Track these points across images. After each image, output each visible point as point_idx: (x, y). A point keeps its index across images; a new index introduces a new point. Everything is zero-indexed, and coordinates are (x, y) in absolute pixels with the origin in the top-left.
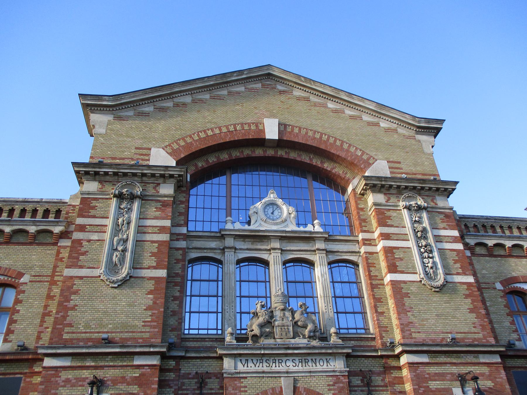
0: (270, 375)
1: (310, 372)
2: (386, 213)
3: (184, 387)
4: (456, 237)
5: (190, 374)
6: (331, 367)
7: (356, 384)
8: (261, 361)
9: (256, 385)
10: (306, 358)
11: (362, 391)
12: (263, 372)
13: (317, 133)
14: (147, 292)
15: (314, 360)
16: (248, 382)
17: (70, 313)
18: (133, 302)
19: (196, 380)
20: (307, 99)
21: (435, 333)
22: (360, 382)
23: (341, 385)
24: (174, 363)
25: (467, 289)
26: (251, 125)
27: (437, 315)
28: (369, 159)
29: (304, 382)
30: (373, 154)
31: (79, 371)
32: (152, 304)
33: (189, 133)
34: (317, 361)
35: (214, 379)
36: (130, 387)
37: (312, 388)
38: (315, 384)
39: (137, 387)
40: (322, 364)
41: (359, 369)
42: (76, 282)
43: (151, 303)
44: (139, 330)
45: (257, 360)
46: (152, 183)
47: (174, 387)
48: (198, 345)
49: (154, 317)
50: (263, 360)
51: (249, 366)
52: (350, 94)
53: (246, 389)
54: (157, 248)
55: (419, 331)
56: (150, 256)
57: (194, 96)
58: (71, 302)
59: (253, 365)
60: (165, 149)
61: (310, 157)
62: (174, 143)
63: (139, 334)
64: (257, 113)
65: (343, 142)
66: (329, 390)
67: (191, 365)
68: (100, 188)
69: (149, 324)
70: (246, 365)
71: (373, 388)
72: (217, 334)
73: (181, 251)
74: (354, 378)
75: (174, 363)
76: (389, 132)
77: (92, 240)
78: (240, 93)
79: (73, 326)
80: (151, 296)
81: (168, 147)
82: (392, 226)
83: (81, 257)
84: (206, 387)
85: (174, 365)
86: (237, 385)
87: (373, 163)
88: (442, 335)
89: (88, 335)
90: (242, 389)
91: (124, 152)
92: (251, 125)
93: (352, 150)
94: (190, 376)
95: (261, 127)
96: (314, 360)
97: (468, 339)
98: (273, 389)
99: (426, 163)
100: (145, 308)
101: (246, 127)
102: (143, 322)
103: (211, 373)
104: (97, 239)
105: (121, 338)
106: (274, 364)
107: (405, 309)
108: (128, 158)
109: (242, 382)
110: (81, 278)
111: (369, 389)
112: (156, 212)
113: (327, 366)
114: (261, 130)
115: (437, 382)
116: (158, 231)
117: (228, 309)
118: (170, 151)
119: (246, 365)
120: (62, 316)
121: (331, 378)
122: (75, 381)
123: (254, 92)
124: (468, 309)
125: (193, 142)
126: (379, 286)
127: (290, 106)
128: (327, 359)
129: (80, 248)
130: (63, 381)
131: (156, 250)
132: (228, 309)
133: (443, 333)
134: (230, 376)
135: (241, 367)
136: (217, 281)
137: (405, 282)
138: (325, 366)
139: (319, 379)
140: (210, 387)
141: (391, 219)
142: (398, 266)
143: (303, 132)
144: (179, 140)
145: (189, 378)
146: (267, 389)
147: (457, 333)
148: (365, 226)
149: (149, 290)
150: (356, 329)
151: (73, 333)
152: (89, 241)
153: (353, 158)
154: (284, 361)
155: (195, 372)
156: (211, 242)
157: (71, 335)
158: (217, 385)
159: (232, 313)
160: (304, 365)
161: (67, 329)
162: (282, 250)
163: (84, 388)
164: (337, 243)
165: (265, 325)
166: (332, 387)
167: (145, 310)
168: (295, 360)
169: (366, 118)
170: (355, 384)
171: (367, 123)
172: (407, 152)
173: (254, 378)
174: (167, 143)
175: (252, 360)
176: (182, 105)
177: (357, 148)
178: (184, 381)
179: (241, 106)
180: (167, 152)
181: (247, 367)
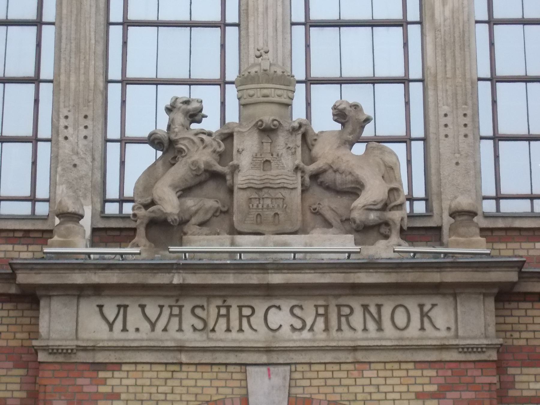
0: (207, 358)
1: (355, 349)
7: (533, 393)
8: (176, 311)
9: (154, 390)
10: (342, 301)
12: (181, 349)
15: (373, 309)
16: (125, 382)
23: (469, 395)
29: (329, 382)
34: (386, 312)
35: (8, 369)
38: (372, 389)
40: (401, 318)
45: (161, 307)
50: (181, 307)
51: (129, 326)
59: (145, 326)
70: (118, 325)
72: (33, 217)
74: (525, 370)
86: (86, 389)
96: (373, 309)
109: (104, 382)
113: (422, 328)
117: (70, 129)
119: (118, 325)
121: (433, 373)
128: (421, 306)
134: (60, 359)
136: (38, 23)
138: (413, 331)
139: (389, 374)
158: (17, 387)
159: (82, 143)
160: (334, 322)
165: (200, 184)
168: (301, 307)
170: (526, 393)
173: (147, 367)
175: (143, 307)
181: (125, 329)
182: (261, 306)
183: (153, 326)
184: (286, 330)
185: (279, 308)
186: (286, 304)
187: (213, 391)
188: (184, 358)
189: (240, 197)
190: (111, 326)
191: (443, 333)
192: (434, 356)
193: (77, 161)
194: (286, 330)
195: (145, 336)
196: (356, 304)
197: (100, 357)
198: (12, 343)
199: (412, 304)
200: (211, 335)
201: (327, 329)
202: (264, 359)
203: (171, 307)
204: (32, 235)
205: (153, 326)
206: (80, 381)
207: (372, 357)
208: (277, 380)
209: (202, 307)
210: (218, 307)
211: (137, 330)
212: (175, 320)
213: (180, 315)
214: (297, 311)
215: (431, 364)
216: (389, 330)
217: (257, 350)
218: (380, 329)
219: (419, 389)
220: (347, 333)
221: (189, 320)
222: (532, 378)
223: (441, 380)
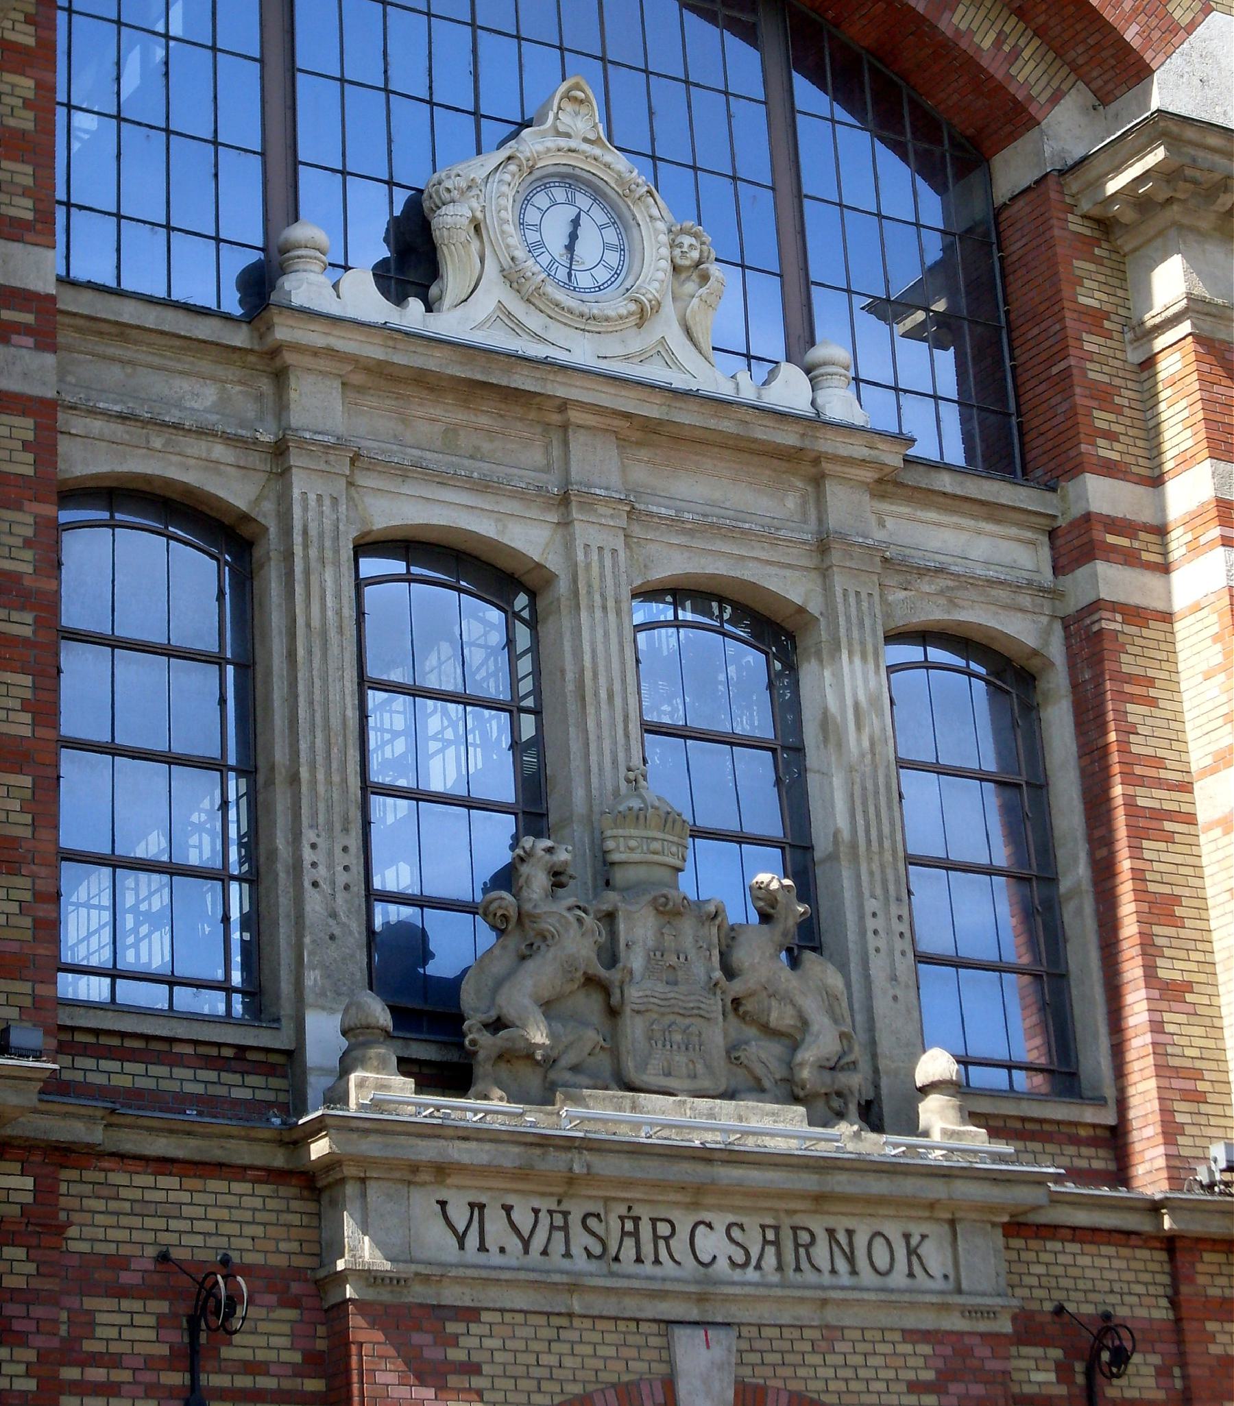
3: (89, 1346)
5: (119, 1263)
15: (842, 1238)
16: (488, 1343)
19: (163, 1307)
22: (1052, 1377)
23: (977, 1390)
24: (29, 1183)
35: (270, 1308)
41: (1048, 1306)
47: (39, 1341)
48: (126, 1082)
51: (489, 1244)
59: (514, 1244)
67: (127, 1206)
70: (472, 1240)
73: (29, 422)
75: (29, 1183)
84: (226, 1352)
85: (29, 1198)
87: (1191, 28)
94: (126, 1278)
96: (842, 1238)
106: (629, 1243)
109: (454, 1341)
113: (911, 1275)
117: (322, 871)
119: (472, 1240)
121: (926, 1349)
126: (1168, 826)
132: (322, 871)
138: (898, 1278)
140: (247, 1355)
145: (122, 1292)
146: (590, 1388)
148: (1111, 436)
150: (172, 982)
155: (151, 1252)
158: (284, 1342)
160: (789, 1256)
164: (932, 515)
168: (741, 1227)
175: (508, 1209)
178: (90, 1303)
181: (482, 1248)
183: (526, 1244)
184: (722, 1264)
185: (709, 1226)
187: (621, 1366)
189: (634, 1029)
190: (461, 1240)
191: (939, 1284)
192: (927, 1321)
193: (337, 931)
194: (722, 1264)
195: (514, 1263)
197: (453, 1295)
198: (274, 1260)
200: (615, 1267)
201: (780, 1268)
202: (694, 1315)
203: (550, 1212)
204: (251, 1056)
205: (526, 1244)
208: (718, 1353)
209: (598, 1216)
210: (622, 1218)
211: (502, 1250)
212: (559, 1236)
213: (565, 1228)
214: (736, 1233)
215: (926, 1336)
216: (867, 1276)
217: (686, 1296)
218: (854, 1272)
219: (911, 1375)
220: (809, 1276)
221: (580, 1239)
222: (1032, 1364)
223: (940, 1363)
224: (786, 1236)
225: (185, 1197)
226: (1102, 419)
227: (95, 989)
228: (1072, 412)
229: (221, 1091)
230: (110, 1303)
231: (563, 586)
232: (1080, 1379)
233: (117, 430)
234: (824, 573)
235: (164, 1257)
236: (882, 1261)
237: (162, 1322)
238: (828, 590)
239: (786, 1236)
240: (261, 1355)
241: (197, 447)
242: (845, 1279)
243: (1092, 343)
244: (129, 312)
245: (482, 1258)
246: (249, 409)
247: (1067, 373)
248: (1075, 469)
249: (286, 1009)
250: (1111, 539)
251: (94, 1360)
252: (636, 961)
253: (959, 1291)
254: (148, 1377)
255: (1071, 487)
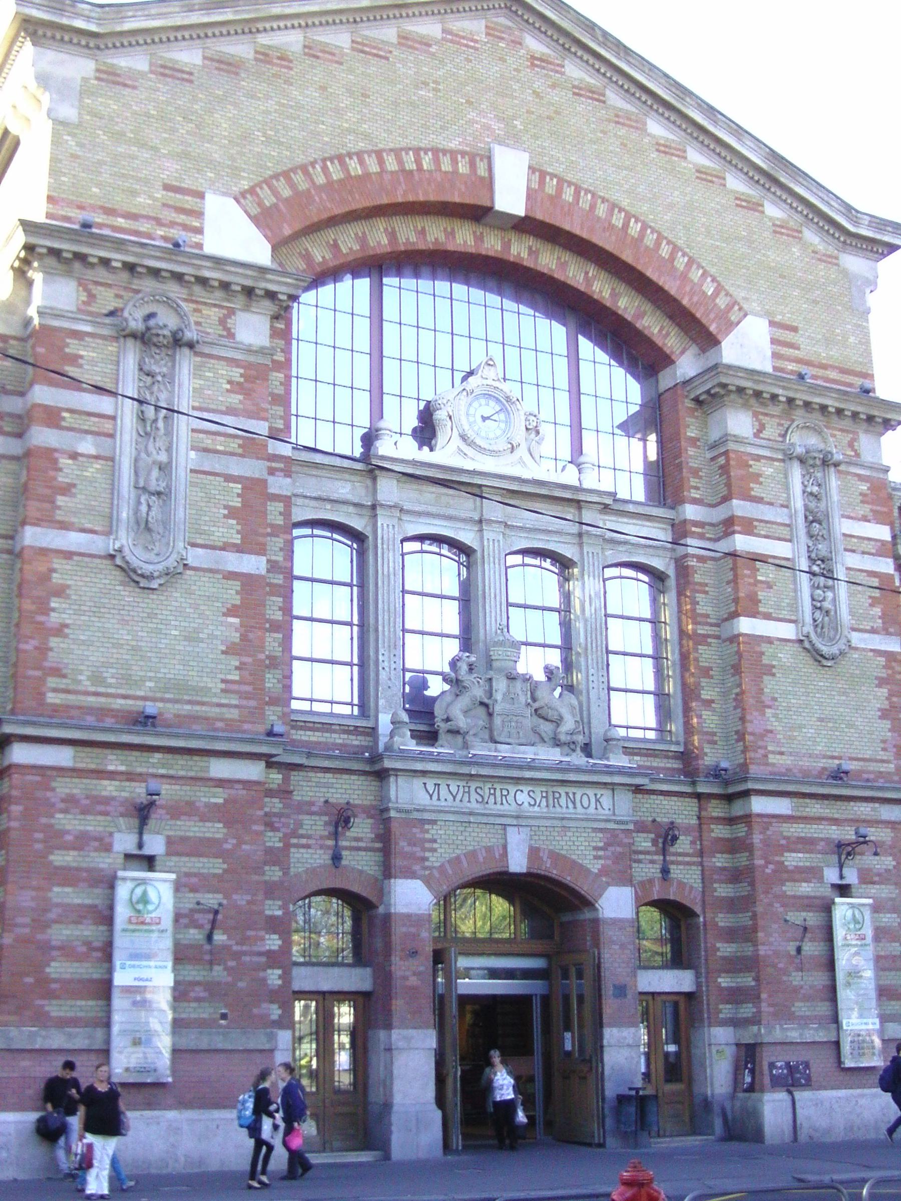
0: (484, 820)
1: (563, 819)
2: (751, 466)
3: (301, 832)
4: (883, 543)
5: (312, 804)
6: (603, 812)
10: (555, 789)
11: (652, 862)
13: (616, 210)
14: (225, 610)
15: (571, 796)
17: (54, 642)
18: (197, 631)
19: (326, 818)
20: (597, 97)
21: (810, 756)
23: (619, 849)
24: (280, 776)
25: (884, 667)
26: (459, 157)
27: (821, 720)
28: (730, 308)
30: (739, 294)
31: (95, 782)
32: (238, 640)
33: (301, 159)
36: (207, 824)
37: (563, 852)
39: (221, 825)
41: (650, 819)
42: (58, 563)
43: (235, 637)
44: (215, 700)
46: (215, 305)
47: (283, 830)
49: (246, 673)
52: (710, 111)
53: (435, 846)
54: (239, 495)
55: (783, 749)
56: (225, 516)
57: (310, 33)
58: (53, 614)
59: (450, 798)
60: (242, 201)
61: (587, 273)
62: (265, 186)
63: (217, 710)
64: (472, 122)
65: (675, 249)
66: (596, 858)
68: (84, 302)
69: (235, 687)
70: (435, 797)
71: (673, 858)
73: (282, 504)
75: (280, 776)
76: (782, 234)
77: (82, 455)
78: (429, 45)
79: (64, 676)
80: (235, 621)
81: (248, 196)
82: (759, 500)
83: (61, 500)
84: (348, 834)
87: (738, 323)
88: (822, 763)
89: (102, 700)
90: (427, 845)
91: (134, 193)
92: (459, 157)
93: (695, 275)
94: (314, 809)
95: (482, 171)
96: (571, 796)
97: (869, 772)
98: (489, 849)
99: (852, 339)
100: (224, 648)
101: (446, 165)
102: (223, 681)
103: (355, 806)
104: (93, 451)
105: (178, 716)
106: (492, 797)
107: (763, 702)
108: (148, 218)
109: (427, 831)
110: (68, 555)
111: (664, 860)
112: (233, 395)
114: (482, 179)
115: (800, 855)
116: (240, 451)
117: (386, 664)
118: (255, 211)
119: (435, 797)
120: (36, 648)
121: (601, 835)
122: (88, 802)
123: (467, 46)
124: (880, 710)
125: (313, 192)
126: (709, 640)
127: (557, 113)
129: (52, 473)
130: (63, 800)
131: (237, 503)
132: (386, 664)
133: (825, 757)
135: (422, 799)
137: (769, 640)
138: (592, 810)
141: (761, 483)
142: (760, 601)
143: (585, 201)
144: (276, 176)
147: (851, 759)
148: (697, 488)
149: (229, 606)
151: (68, 691)
152: (74, 456)
153: (695, 299)
154: (512, 794)
155: (322, 800)
156: (339, 484)
157: (63, 696)
159: (393, 672)
160: (551, 802)
161: (52, 682)
162: (506, 525)
163: (109, 818)
164: (625, 520)
166: (601, 853)
167: (223, 652)
169: (735, 183)
171: (737, 199)
172: (815, 302)
174: (245, 185)
176: (279, 58)
177: (705, 274)
178: (301, 817)
179: (434, 89)
180: (246, 212)
181: (439, 799)
182: (512, 789)
183: (454, 798)
184: (526, 804)
186: (526, 789)
188: (472, 819)
189: (498, 721)
190: (431, 796)
191: (607, 812)
192: (602, 825)
196: (562, 790)
197: (426, 816)
198: (365, 803)
199: (591, 792)
202: (515, 823)
205: (454, 798)
206: (414, 830)
207: (571, 824)
208: (523, 836)
213: (469, 792)
215: (601, 830)
216: (580, 809)
217: (512, 817)
218: (575, 808)
220: (558, 809)
221: (474, 796)
224: (550, 794)
225: (334, 781)
226: (693, 482)
227: (304, 706)
228: (681, 479)
229: (349, 742)
230: (308, 817)
231: (479, 554)
232: (661, 845)
233: (313, 503)
234: (581, 545)
235: (326, 802)
236: (586, 804)
237: (326, 824)
238: (582, 553)
239: (550, 794)
240: (360, 835)
241: (344, 508)
242: (571, 810)
243: (691, 451)
244: (318, 458)
245: (438, 803)
246: (363, 492)
247: (681, 463)
248: (682, 501)
249: (372, 713)
250: (694, 529)
251: (302, 836)
252: (499, 696)
253: (614, 814)
254: (320, 842)
255: (680, 508)
